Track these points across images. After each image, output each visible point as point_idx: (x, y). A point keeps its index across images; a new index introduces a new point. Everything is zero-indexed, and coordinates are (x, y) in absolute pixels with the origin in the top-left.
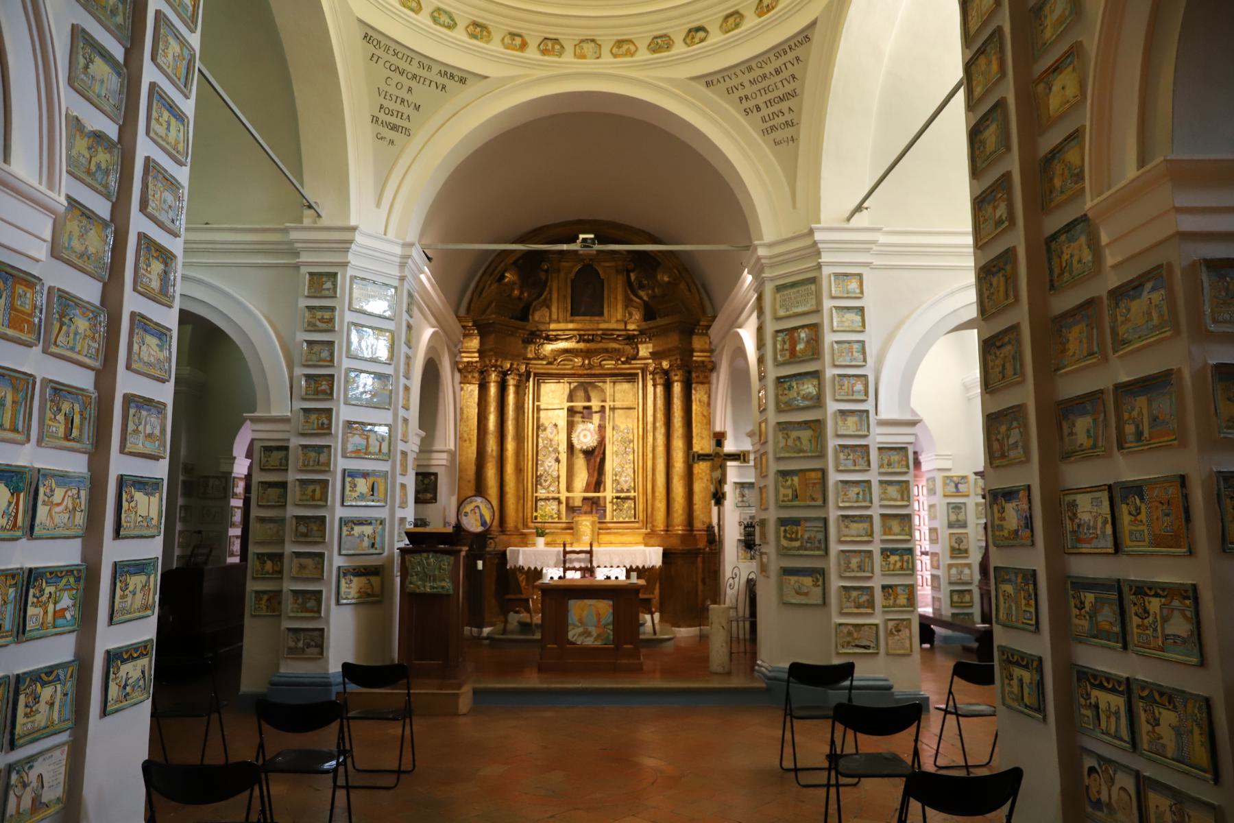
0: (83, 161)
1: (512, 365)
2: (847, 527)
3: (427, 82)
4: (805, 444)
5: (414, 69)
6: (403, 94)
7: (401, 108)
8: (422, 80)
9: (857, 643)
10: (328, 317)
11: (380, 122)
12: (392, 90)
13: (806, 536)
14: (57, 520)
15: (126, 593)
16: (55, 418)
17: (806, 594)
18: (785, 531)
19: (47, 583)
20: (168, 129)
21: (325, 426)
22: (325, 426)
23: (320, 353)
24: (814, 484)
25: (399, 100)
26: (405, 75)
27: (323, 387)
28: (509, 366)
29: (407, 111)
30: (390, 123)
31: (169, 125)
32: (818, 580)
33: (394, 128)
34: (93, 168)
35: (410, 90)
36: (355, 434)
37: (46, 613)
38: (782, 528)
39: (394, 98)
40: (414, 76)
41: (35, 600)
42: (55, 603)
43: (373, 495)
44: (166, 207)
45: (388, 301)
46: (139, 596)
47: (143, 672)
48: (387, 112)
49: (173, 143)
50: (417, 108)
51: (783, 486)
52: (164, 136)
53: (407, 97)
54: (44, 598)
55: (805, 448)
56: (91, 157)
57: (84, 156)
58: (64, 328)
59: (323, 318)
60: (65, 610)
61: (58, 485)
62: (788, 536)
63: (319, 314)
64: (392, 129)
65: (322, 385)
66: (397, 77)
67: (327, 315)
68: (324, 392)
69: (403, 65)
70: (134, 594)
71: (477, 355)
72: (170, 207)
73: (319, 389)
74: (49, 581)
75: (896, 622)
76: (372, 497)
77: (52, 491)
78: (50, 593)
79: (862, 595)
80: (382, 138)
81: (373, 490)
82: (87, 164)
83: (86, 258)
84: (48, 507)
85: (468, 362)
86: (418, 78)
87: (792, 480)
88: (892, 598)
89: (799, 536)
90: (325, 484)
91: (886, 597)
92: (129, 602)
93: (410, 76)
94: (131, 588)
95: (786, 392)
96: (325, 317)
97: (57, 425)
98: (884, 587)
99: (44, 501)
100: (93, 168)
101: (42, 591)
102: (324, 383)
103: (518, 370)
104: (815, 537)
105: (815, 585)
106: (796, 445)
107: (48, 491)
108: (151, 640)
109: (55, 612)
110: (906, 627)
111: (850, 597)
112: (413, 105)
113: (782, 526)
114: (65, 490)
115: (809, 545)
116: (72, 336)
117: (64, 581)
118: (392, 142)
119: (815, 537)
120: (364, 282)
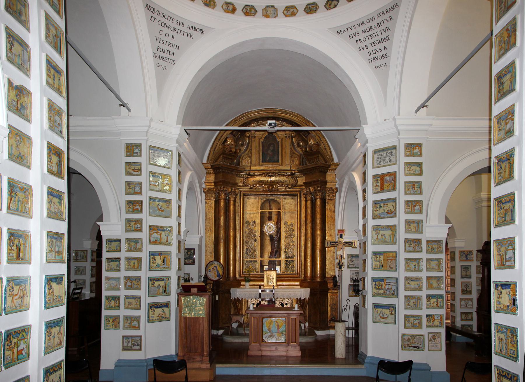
0: (14, 103)
1: (232, 189)
2: (409, 283)
4: (388, 239)
9: (412, 345)
13: (387, 287)
14: (16, 303)
15: (50, 338)
16: (12, 248)
17: (386, 318)
18: (376, 284)
19: (13, 337)
20: (54, 79)
21: (139, 228)
22: (139, 228)
24: (392, 260)
27: (137, 207)
28: (230, 190)
31: (54, 77)
32: (392, 311)
34: (19, 107)
36: (154, 232)
37: (13, 353)
38: (374, 283)
41: (8, 347)
42: (17, 347)
44: (57, 125)
45: (168, 159)
46: (57, 338)
47: (60, 378)
49: (57, 87)
51: (375, 260)
52: (52, 83)
54: (12, 346)
55: (387, 241)
56: (18, 101)
57: (14, 101)
58: (13, 199)
60: (22, 350)
61: (15, 284)
62: (378, 287)
68: (137, 209)
70: (54, 338)
71: (213, 184)
72: (59, 124)
73: (135, 208)
74: (14, 336)
75: (433, 334)
77: (13, 288)
78: (15, 342)
79: (416, 319)
82: (16, 105)
83: (20, 159)
84: (12, 297)
85: (209, 188)
87: (380, 257)
88: (431, 321)
89: (383, 288)
90: (139, 259)
91: (428, 321)
92: (52, 342)
94: (53, 335)
95: (378, 209)
97: (12, 252)
98: (427, 316)
99: (9, 294)
100: (19, 107)
101: (11, 342)
102: (137, 205)
103: (235, 192)
104: (391, 288)
105: (391, 314)
106: (382, 238)
107: (11, 289)
108: (63, 360)
109: (18, 352)
110: (438, 337)
111: (409, 321)
113: (374, 282)
114: (19, 287)
115: (388, 292)
116: (17, 202)
117: (21, 335)
119: (391, 288)
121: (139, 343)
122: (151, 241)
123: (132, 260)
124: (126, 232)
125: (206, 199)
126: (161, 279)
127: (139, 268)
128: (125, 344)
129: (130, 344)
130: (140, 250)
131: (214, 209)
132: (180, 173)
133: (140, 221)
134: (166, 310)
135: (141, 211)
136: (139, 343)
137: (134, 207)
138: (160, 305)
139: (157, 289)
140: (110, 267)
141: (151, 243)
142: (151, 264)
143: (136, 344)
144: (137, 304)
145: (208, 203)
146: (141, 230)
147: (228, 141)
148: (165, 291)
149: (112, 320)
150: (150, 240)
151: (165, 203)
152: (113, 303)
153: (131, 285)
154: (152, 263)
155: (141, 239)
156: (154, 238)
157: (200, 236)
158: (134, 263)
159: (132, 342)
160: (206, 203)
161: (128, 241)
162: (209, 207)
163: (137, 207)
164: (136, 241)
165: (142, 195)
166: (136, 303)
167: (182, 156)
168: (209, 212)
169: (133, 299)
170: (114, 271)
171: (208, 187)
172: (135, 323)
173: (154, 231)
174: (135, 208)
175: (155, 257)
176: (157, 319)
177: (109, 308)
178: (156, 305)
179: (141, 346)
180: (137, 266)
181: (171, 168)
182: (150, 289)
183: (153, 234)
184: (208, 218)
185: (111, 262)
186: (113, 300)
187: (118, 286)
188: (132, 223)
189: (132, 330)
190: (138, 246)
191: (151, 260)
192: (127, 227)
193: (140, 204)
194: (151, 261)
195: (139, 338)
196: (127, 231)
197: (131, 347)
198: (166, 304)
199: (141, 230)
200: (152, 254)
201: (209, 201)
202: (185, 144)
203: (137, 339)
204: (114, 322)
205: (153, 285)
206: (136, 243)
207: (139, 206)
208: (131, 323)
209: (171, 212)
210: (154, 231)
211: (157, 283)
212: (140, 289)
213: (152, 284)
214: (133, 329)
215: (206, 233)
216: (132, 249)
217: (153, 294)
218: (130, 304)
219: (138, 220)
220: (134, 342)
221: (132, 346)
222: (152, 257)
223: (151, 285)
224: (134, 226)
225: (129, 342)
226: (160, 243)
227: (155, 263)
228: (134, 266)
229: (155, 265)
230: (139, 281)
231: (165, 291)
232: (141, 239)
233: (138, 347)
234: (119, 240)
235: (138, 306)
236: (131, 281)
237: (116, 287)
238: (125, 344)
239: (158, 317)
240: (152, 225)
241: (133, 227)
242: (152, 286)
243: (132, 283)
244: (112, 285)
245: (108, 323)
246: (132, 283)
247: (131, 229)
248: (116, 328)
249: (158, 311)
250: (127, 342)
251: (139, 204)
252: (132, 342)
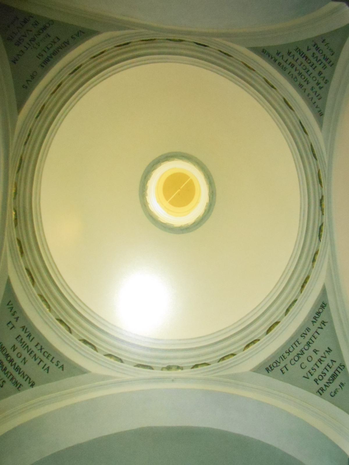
3: (316, 335)
5: (304, 341)
6: (316, 357)
29: (327, 361)
30: (329, 380)
33: (334, 377)
35: (315, 351)
40: (308, 344)
66: (303, 359)
69: (297, 350)
80: (335, 393)
86: (311, 341)
93: (306, 347)
118: (342, 385)
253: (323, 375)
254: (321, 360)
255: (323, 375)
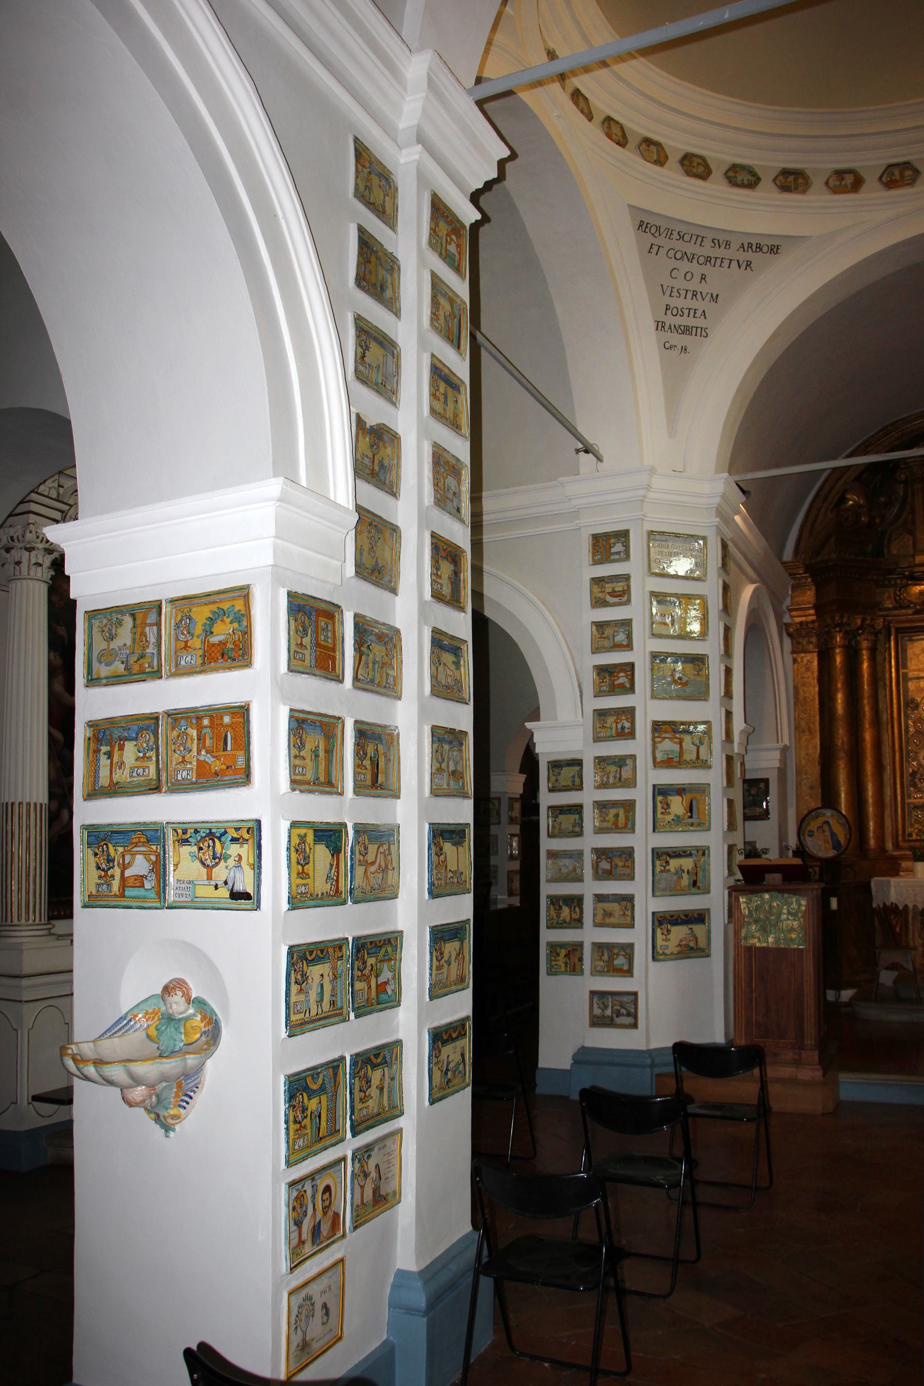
3: (726, 263)
5: (707, 250)
6: (694, 285)
7: (693, 304)
8: (719, 261)
10: (621, 589)
11: (667, 327)
12: (680, 284)
21: (626, 731)
22: (626, 731)
23: (614, 637)
25: (690, 295)
26: (695, 261)
30: (680, 326)
33: (686, 330)
35: (703, 278)
39: (683, 293)
40: (708, 260)
43: (691, 817)
45: (695, 557)
48: (675, 312)
50: (715, 298)
53: (700, 288)
59: (614, 591)
63: (609, 587)
64: (683, 333)
65: (619, 678)
66: (685, 266)
67: (619, 587)
68: (622, 685)
69: (691, 249)
73: (616, 683)
76: (690, 820)
81: (691, 811)
86: (713, 261)
90: (630, 806)
93: (702, 260)
96: (616, 589)
102: (622, 674)
112: (709, 295)
118: (684, 349)
120: (663, 538)
121: (632, 1010)
122: (658, 760)
123: (611, 808)
124: (594, 741)
125: (793, 652)
126: (685, 852)
127: (629, 826)
128: (597, 1011)
129: (608, 1012)
130: (631, 783)
131: (816, 674)
132: (726, 588)
133: (630, 712)
134: (698, 929)
135: (632, 690)
136: (632, 1010)
137: (614, 681)
138: (683, 917)
139: (675, 878)
140: (558, 827)
141: (656, 764)
142: (659, 816)
143: (623, 1011)
144: (624, 914)
145: (799, 660)
146: (631, 735)
147: (850, 500)
148: (695, 883)
149: (563, 952)
150: (654, 758)
151: (691, 665)
152: (566, 911)
153: (609, 868)
154: (662, 813)
155: (633, 757)
156: (666, 753)
157: (781, 745)
158: (617, 816)
159: (615, 1008)
160: (795, 661)
161: (599, 763)
162: (803, 670)
163: (622, 679)
164: (620, 761)
165: (632, 649)
166: (622, 913)
167: (731, 547)
168: (804, 685)
169: (614, 902)
170: (568, 837)
171: (798, 620)
172: (620, 961)
173: (664, 735)
174: (616, 683)
175: (670, 798)
176: (675, 952)
177: (557, 923)
178: (672, 916)
179: (635, 1017)
180: (623, 821)
181: (703, 578)
182: (657, 878)
183: (660, 742)
184: (802, 698)
185: (561, 816)
186: (567, 905)
187: (578, 871)
188: (610, 720)
189: (613, 976)
190: (626, 773)
191: (659, 806)
192: (598, 730)
193: (629, 673)
194: (659, 810)
195: (632, 997)
196: (597, 739)
197: (612, 1019)
198: (700, 915)
199: (631, 735)
200: (661, 791)
201: (803, 655)
202: (737, 518)
203: (625, 999)
204: (569, 959)
205: (665, 867)
206: (620, 767)
207: (627, 677)
208: (611, 959)
209: (707, 686)
210: (664, 735)
211: (674, 864)
212: (633, 878)
213: (661, 866)
214: (615, 974)
215: (798, 739)
216: (611, 781)
217: (663, 890)
218: (608, 914)
219: (623, 712)
220: (618, 1008)
221: (614, 1016)
222: (660, 798)
223: (658, 869)
224: (614, 725)
225: (606, 1007)
226: (679, 762)
227: (669, 813)
228: (616, 824)
229: (669, 818)
230: (630, 857)
231: (695, 883)
232: (633, 757)
233: (628, 1020)
234: (578, 763)
235: (629, 920)
236: (610, 858)
237: (573, 874)
238: (597, 1011)
239: (679, 949)
240: (659, 722)
241: (611, 729)
242: (661, 871)
243: (611, 863)
244: (564, 870)
245: (556, 960)
246: (611, 863)
247: (608, 734)
248: (574, 971)
249: (679, 933)
250: (602, 1006)
251: (625, 671)
252: (615, 1008)
253: (680, 312)
254: (696, 295)
255: (680, 312)
